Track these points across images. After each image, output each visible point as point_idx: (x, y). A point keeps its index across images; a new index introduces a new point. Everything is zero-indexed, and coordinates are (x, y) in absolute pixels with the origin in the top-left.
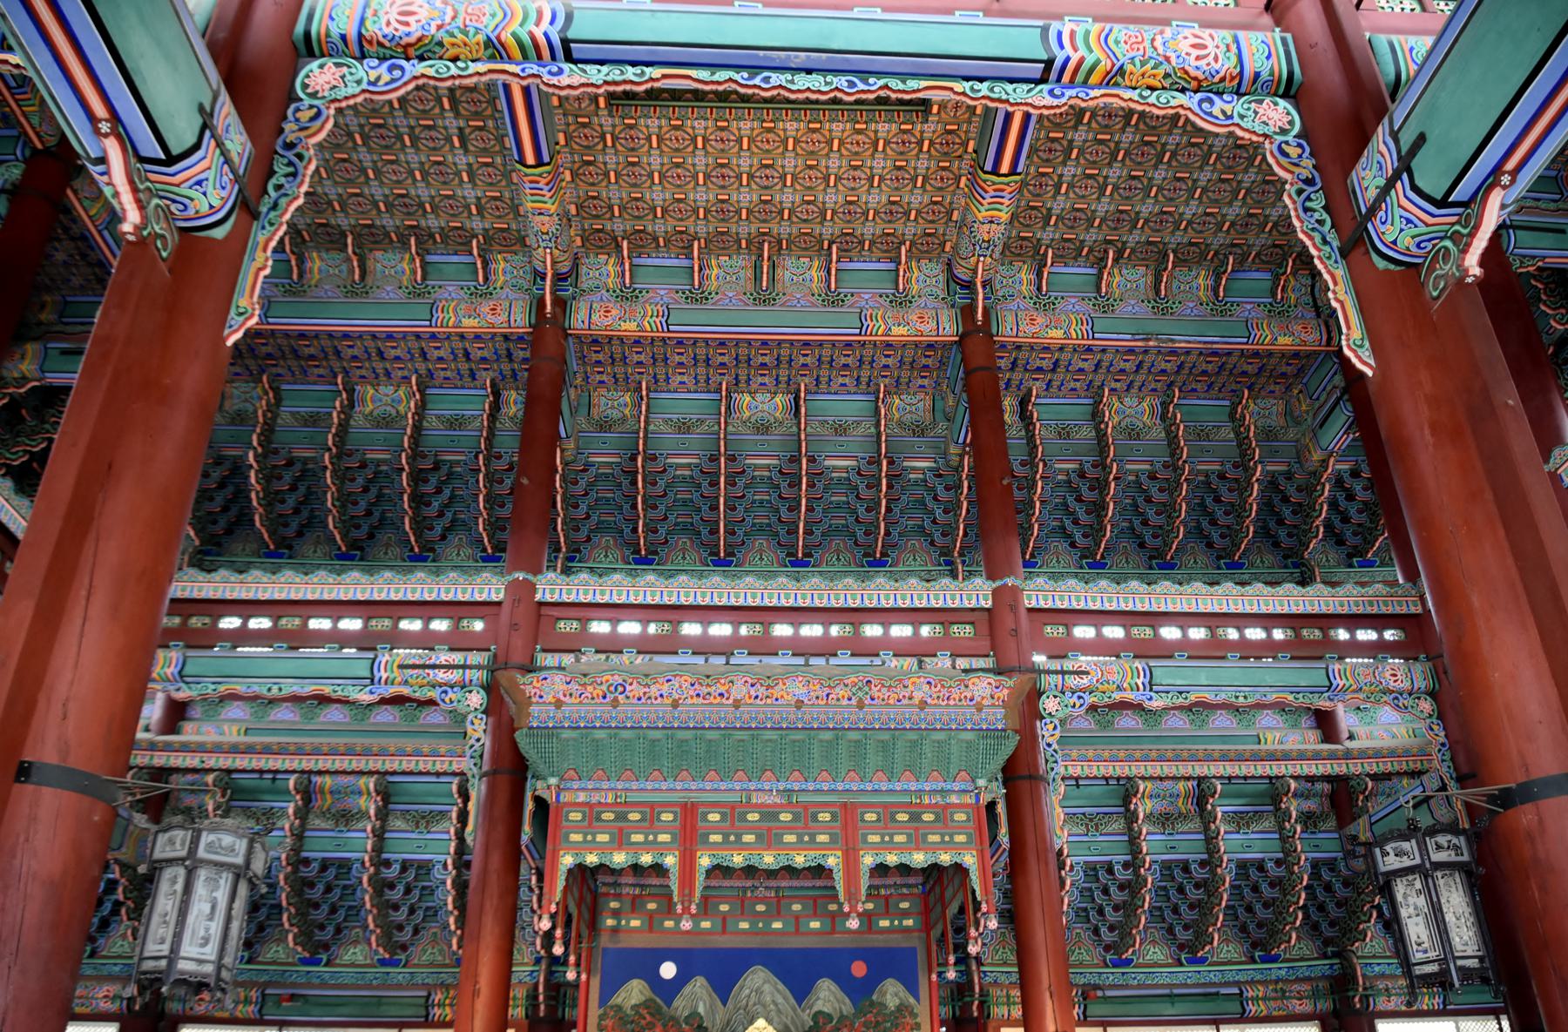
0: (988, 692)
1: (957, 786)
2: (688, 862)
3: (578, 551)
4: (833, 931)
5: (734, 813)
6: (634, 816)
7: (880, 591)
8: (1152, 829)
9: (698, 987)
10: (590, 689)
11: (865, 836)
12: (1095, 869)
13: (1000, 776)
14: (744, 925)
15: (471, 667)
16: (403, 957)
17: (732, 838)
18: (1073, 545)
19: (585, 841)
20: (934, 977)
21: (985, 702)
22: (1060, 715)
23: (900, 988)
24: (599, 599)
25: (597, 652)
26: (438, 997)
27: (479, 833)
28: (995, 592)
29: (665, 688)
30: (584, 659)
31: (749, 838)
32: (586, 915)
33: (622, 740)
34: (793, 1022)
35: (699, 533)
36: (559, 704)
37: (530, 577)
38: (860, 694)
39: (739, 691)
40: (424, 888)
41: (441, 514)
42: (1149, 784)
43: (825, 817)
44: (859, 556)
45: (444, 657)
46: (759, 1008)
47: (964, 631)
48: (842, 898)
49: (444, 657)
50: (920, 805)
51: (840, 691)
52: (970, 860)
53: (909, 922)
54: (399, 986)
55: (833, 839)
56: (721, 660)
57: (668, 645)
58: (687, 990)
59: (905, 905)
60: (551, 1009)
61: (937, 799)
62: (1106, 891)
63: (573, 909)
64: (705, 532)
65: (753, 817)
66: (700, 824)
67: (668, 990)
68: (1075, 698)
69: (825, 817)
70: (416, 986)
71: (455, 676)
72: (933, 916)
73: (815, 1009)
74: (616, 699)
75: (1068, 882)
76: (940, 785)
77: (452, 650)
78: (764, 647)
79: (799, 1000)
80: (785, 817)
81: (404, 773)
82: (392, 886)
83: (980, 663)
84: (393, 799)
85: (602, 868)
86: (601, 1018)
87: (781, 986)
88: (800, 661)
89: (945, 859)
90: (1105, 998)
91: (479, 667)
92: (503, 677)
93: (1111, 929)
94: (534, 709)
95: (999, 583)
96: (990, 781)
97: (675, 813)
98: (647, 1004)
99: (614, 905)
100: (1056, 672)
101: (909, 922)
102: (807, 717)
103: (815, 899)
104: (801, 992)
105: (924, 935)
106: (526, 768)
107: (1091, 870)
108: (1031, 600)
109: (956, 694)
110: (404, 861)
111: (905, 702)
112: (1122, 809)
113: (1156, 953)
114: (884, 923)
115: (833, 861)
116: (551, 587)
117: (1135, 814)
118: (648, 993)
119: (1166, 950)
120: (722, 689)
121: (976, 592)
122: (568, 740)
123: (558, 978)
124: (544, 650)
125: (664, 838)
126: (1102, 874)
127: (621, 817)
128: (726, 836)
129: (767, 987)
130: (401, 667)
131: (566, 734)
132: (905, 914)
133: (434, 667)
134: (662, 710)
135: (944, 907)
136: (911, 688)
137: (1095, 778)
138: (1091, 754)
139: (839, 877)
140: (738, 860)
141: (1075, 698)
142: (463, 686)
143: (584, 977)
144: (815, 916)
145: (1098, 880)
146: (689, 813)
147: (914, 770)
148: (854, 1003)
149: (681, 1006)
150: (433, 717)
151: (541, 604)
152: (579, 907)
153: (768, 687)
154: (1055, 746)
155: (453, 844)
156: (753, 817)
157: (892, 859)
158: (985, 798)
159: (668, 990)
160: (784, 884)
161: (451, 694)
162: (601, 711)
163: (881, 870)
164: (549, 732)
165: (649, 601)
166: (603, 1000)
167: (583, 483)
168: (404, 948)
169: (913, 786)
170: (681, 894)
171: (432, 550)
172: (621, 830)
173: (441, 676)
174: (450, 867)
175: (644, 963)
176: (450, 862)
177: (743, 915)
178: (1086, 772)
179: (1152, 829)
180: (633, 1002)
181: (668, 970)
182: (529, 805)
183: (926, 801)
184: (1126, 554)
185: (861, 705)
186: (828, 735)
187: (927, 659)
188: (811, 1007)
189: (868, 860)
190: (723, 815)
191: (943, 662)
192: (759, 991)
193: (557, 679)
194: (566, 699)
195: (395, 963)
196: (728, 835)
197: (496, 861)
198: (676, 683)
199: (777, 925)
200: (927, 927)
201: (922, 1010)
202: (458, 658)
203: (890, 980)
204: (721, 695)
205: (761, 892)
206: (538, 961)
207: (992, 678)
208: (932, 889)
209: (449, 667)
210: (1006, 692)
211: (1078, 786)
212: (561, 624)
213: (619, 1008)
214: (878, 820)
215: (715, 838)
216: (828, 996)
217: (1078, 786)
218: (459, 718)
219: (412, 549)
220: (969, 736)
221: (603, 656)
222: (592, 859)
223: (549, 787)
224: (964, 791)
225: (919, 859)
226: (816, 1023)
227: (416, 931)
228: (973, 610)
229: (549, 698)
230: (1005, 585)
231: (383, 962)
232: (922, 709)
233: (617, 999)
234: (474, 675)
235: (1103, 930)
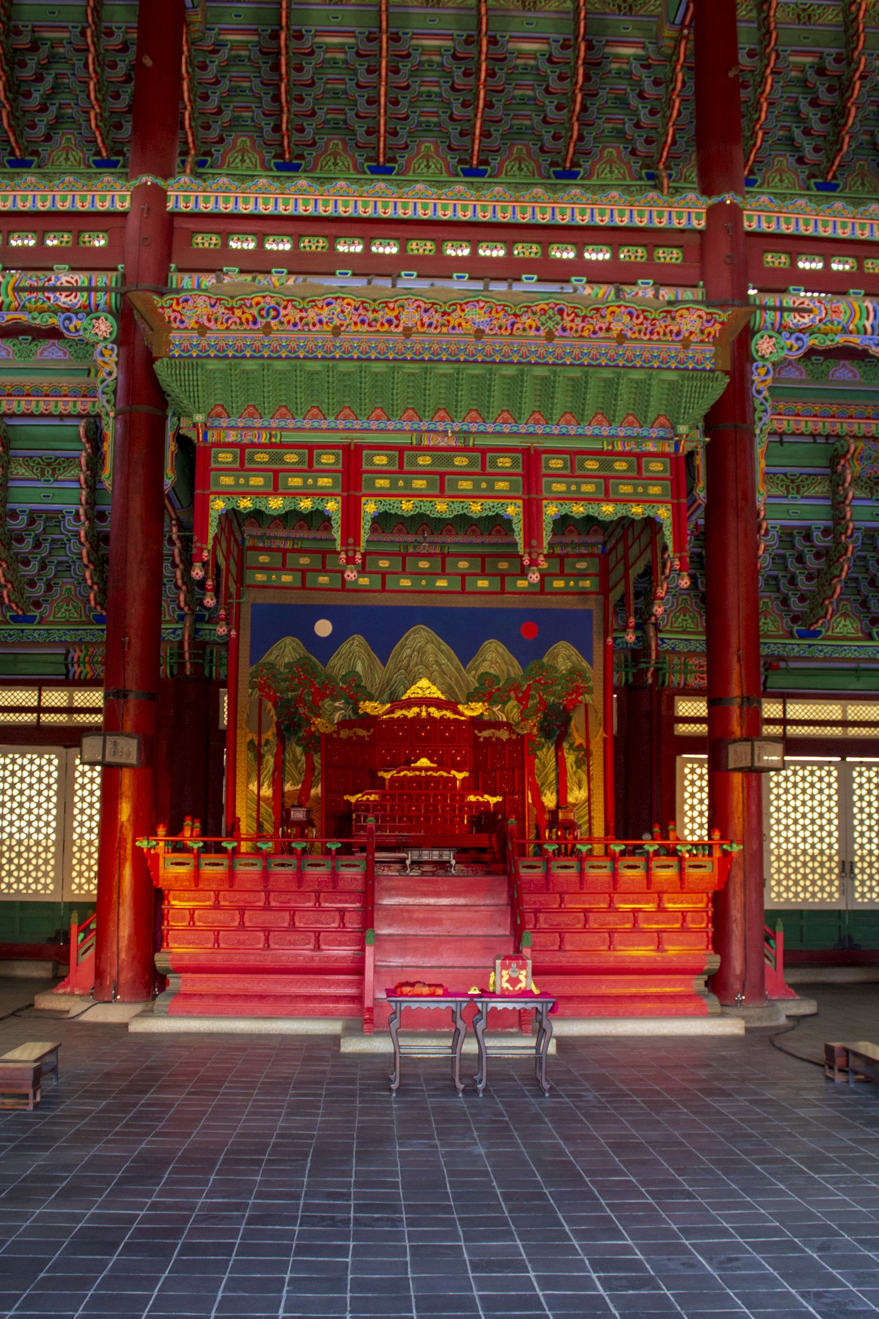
0: (696, 328)
1: (655, 433)
2: (351, 510)
3: (209, 154)
4: (503, 592)
7: (573, 207)
8: (858, 494)
9: (356, 644)
10: (238, 312)
11: (549, 485)
12: (791, 535)
13: (701, 425)
14: (406, 583)
15: (97, 290)
16: (37, 613)
17: (401, 483)
18: (801, 161)
19: (237, 484)
20: (610, 640)
22: (774, 358)
23: (573, 651)
24: (242, 209)
25: (242, 272)
26: (76, 654)
27: (118, 477)
28: (711, 212)
29: (325, 313)
30: (227, 280)
31: (419, 484)
32: (233, 569)
33: (275, 371)
34: (458, 683)
35: (353, 132)
37: (160, 182)
38: (550, 324)
39: (410, 317)
40: (54, 541)
41: (43, 109)
42: (861, 445)
44: (545, 165)
45: (65, 278)
46: (421, 668)
47: (669, 256)
48: (521, 549)
49: (65, 278)
52: (664, 514)
53: (587, 583)
54: (35, 644)
56: (387, 283)
57: (328, 263)
58: (345, 648)
59: (582, 565)
60: (198, 668)
61: (630, 447)
62: (800, 559)
63: (221, 561)
64: (360, 131)
65: (424, 461)
66: (365, 467)
67: (325, 649)
68: (792, 341)
70: (54, 643)
71: (81, 298)
72: (614, 577)
73: (481, 670)
74: (268, 324)
75: (762, 547)
76: (636, 431)
77: (73, 269)
80: (460, 461)
81: (23, 415)
82: (20, 540)
83: (687, 294)
84: (14, 444)
85: (257, 515)
86: (254, 675)
87: (445, 647)
88: (478, 286)
89: (637, 511)
90: (787, 670)
91: (106, 290)
92: (137, 298)
93: (802, 599)
94: (175, 337)
95: (714, 200)
96: (691, 428)
97: (336, 455)
98: (301, 663)
99: (264, 559)
100: (774, 309)
101: (587, 583)
102: (488, 348)
103: (483, 557)
104: (466, 651)
105: (601, 597)
106: (164, 405)
107: (787, 535)
108: (750, 224)
109: (660, 327)
110: (32, 511)
112: (828, 471)
113: (845, 626)
114: (559, 584)
115: (513, 510)
116: (184, 195)
117: (842, 475)
118: (303, 651)
119: (857, 625)
120: (392, 315)
121: (689, 211)
122: (214, 371)
123: (205, 636)
124: (180, 270)
125: (325, 482)
126: (799, 542)
128: (394, 483)
129: (429, 646)
130: (17, 289)
131: (212, 365)
132: (583, 575)
133: (54, 289)
134: (321, 337)
135: (627, 568)
136: (609, 318)
137: (802, 434)
138: (799, 408)
139: (518, 527)
140: (407, 507)
141: (792, 341)
142: (88, 310)
143: (233, 632)
144: (483, 574)
145: (793, 547)
146: (352, 457)
147: (607, 415)
148: (523, 665)
149: (338, 664)
150: (51, 352)
151: (174, 215)
152: (227, 559)
153: (444, 313)
154: (765, 393)
155: (84, 493)
157: (578, 510)
158: (686, 447)
160: (448, 539)
161: (75, 322)
162: (251, 338)
163: (563, 523)
164: (193, 362)
165: (301, 211)
166: (254, 659)
167: (213, 69)
168: (37, 605)
169: (605, 431)
170: (344, 543)
171: (36, 153)
172: (276, 472)
173: (64, 300)
174: (83, 518)
175: (298, 621)
176: (81, 512)
177: (404, 572)
178: (792, 427)
179: (858, 494)
180: (287, 660)
182: (171, 447)
183: (619, 448)
184: (862, 175)
185: (550, 336)
186: (511, 371)
187: (627, 288)
189: (551, 510)
191: (644, 290)
192: (421, 651)
193: (200, 302)
194: (211, 325)
195: (31, 620)
196: (398, 480)
197: (137, 505)
198: (337, 307)
199: (442, 583)
200: (605, 589)
201: (595, 675)
202: (81, 279)
203: (562, 643)
204: (390, 322)
205: (425, 548)
206: (181, 618)
207: (704, 310)
208: (614, 547)
209: (73, 290)
211: (782, 443)
212: (198, 239)
213: (271, 666)
214: (564, 467)
215: (382, 483)
216: (494, 657)
217: (782, 443)
218: (86, 346)
219: (12, 153)
220: (672, 376)
221: (249, 278)
222: (245, 504)
223: (195, 425)
224: (662, 438)
225: (608, 511)
226: (481, 684)
227: (49, 588)
228: (682, 231)
230: (723, 203)
231: (16, 619)
232: (620, 343)
233: (271, 656)
234: (101, 298)
235: (793, 600)
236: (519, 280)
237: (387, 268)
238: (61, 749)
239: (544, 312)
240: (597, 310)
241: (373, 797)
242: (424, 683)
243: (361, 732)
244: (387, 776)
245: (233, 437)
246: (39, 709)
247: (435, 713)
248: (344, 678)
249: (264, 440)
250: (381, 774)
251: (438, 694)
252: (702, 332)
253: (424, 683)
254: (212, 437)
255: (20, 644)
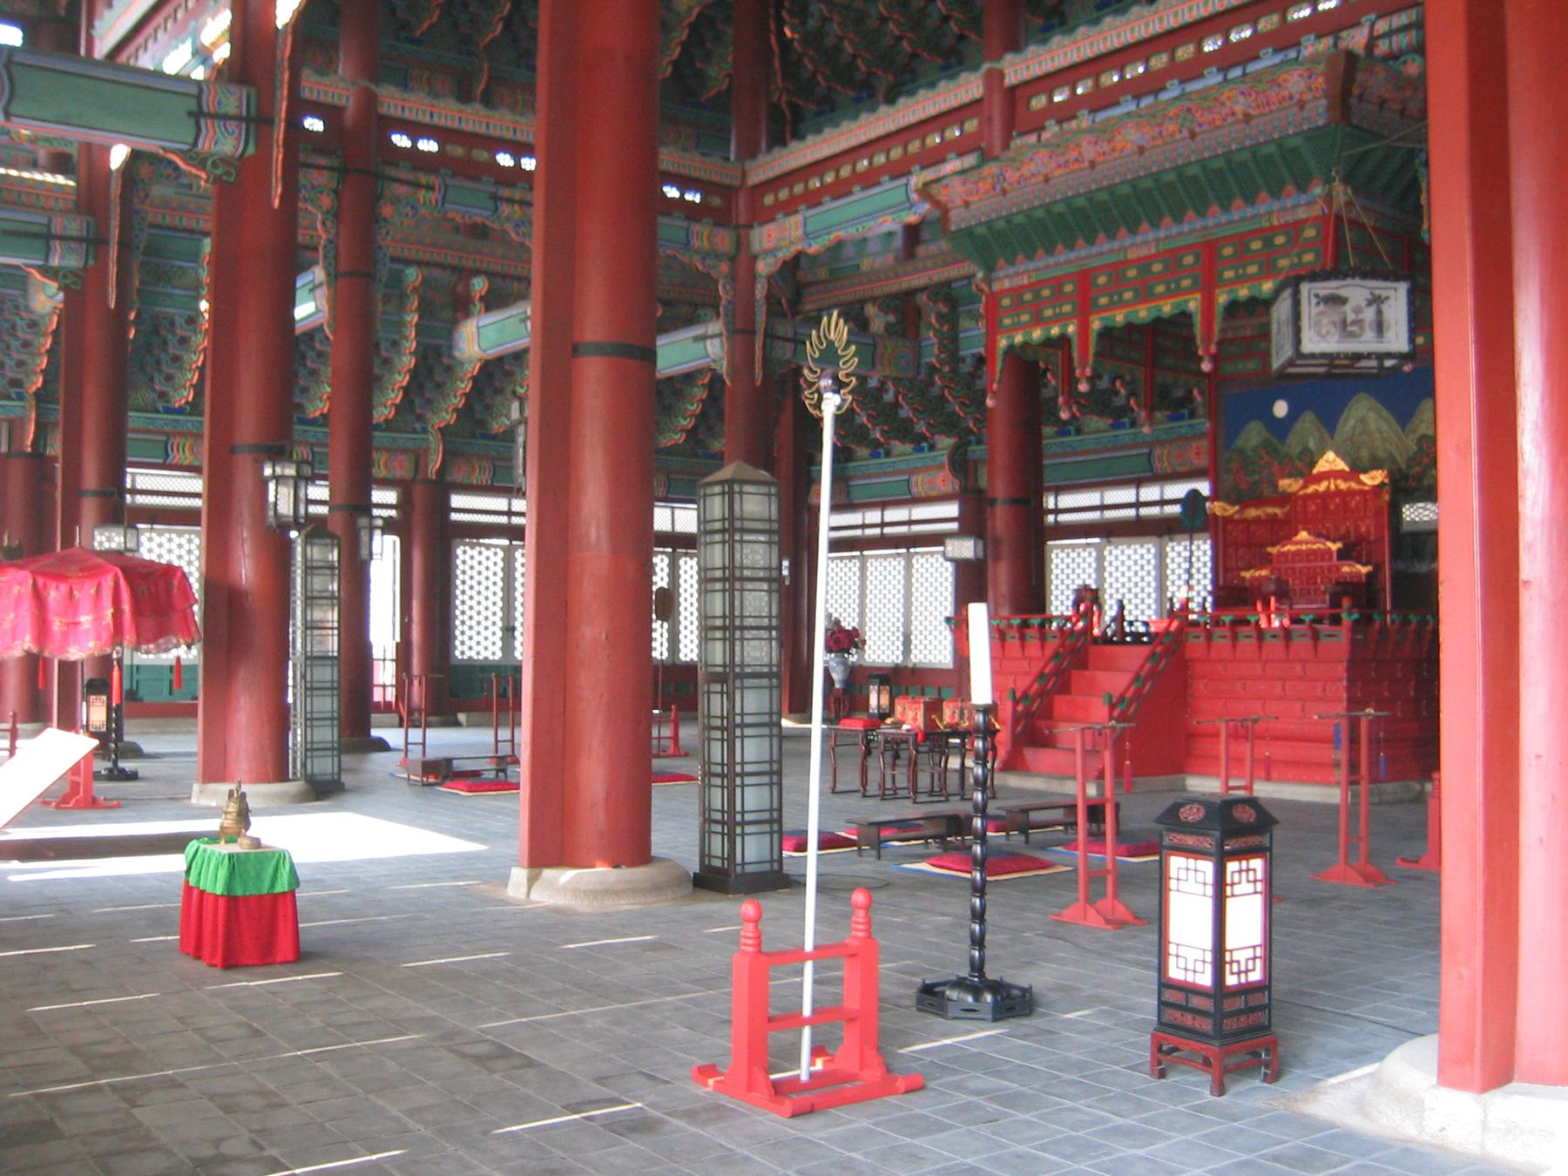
0: (1302, 86)
2: (1084, 328)
5: (1116, 269)
6: (1046, 293)
9: (1308, 421)
21: (1308, 96)
29: (1033, 167)
31: (1128, 295)
36: (967, 204)
39: (1089, 152)
43: (1189, 260)
50: (1272, 228)
51: (1170, 127)
55: (1194, 283)
58: (1298, 426)
67: (1281, 429)
69: (1189, 260)
78: (1102, 100)
79: (1403, 426)
87: (1385, 413)
98: (1265, 445)
111: (1230, 120)
115: (1193, 304)
120: (1075, 154)
125: (1067, 308)
127: (1037, 295)
136: (1228, 103)
139: (1198, 321)
149: (1293, 444)
151: (1013, 88)
156: (1102, 280)
157: (1243, 293)
159: (1281, 429)
181: (1281, 409)
185: (1193, 135)
188: (1414, 431)
189: (1222, 299)
190: (1110, 277)
192: (1363, 420)
195: (1122, 426)
210: (1321, 80)
213: (1241, 451)
215: (1103, 301)
226: (1420, 448)
229: (958, 202)
233: (1239, 443)
236: (1257, 58)
237: (1247, 52)
238: (1155, 539)
239: (1177, 116)
240: (1215, 99)
241: (1264, 573)
242: (1330, 455)
243: (1278, 511)
244: (1273, 550)
245: (1007, 284)
246: (1138, 505)
247: (1343, 485)
248: (1299, 456)
249: (1026, 282)
250: (1269, 549)
251: (1341, 465)
252: (1310, 89)
253: (1330, 455)
254: (996, 287)
255: (1115, 449)
